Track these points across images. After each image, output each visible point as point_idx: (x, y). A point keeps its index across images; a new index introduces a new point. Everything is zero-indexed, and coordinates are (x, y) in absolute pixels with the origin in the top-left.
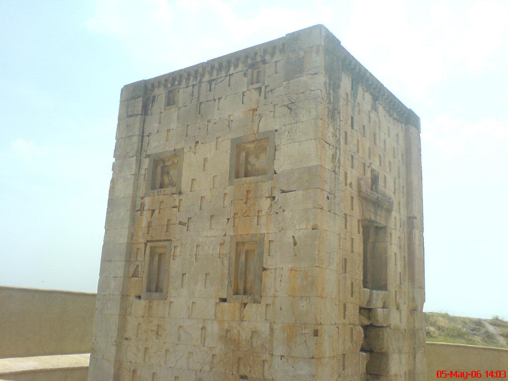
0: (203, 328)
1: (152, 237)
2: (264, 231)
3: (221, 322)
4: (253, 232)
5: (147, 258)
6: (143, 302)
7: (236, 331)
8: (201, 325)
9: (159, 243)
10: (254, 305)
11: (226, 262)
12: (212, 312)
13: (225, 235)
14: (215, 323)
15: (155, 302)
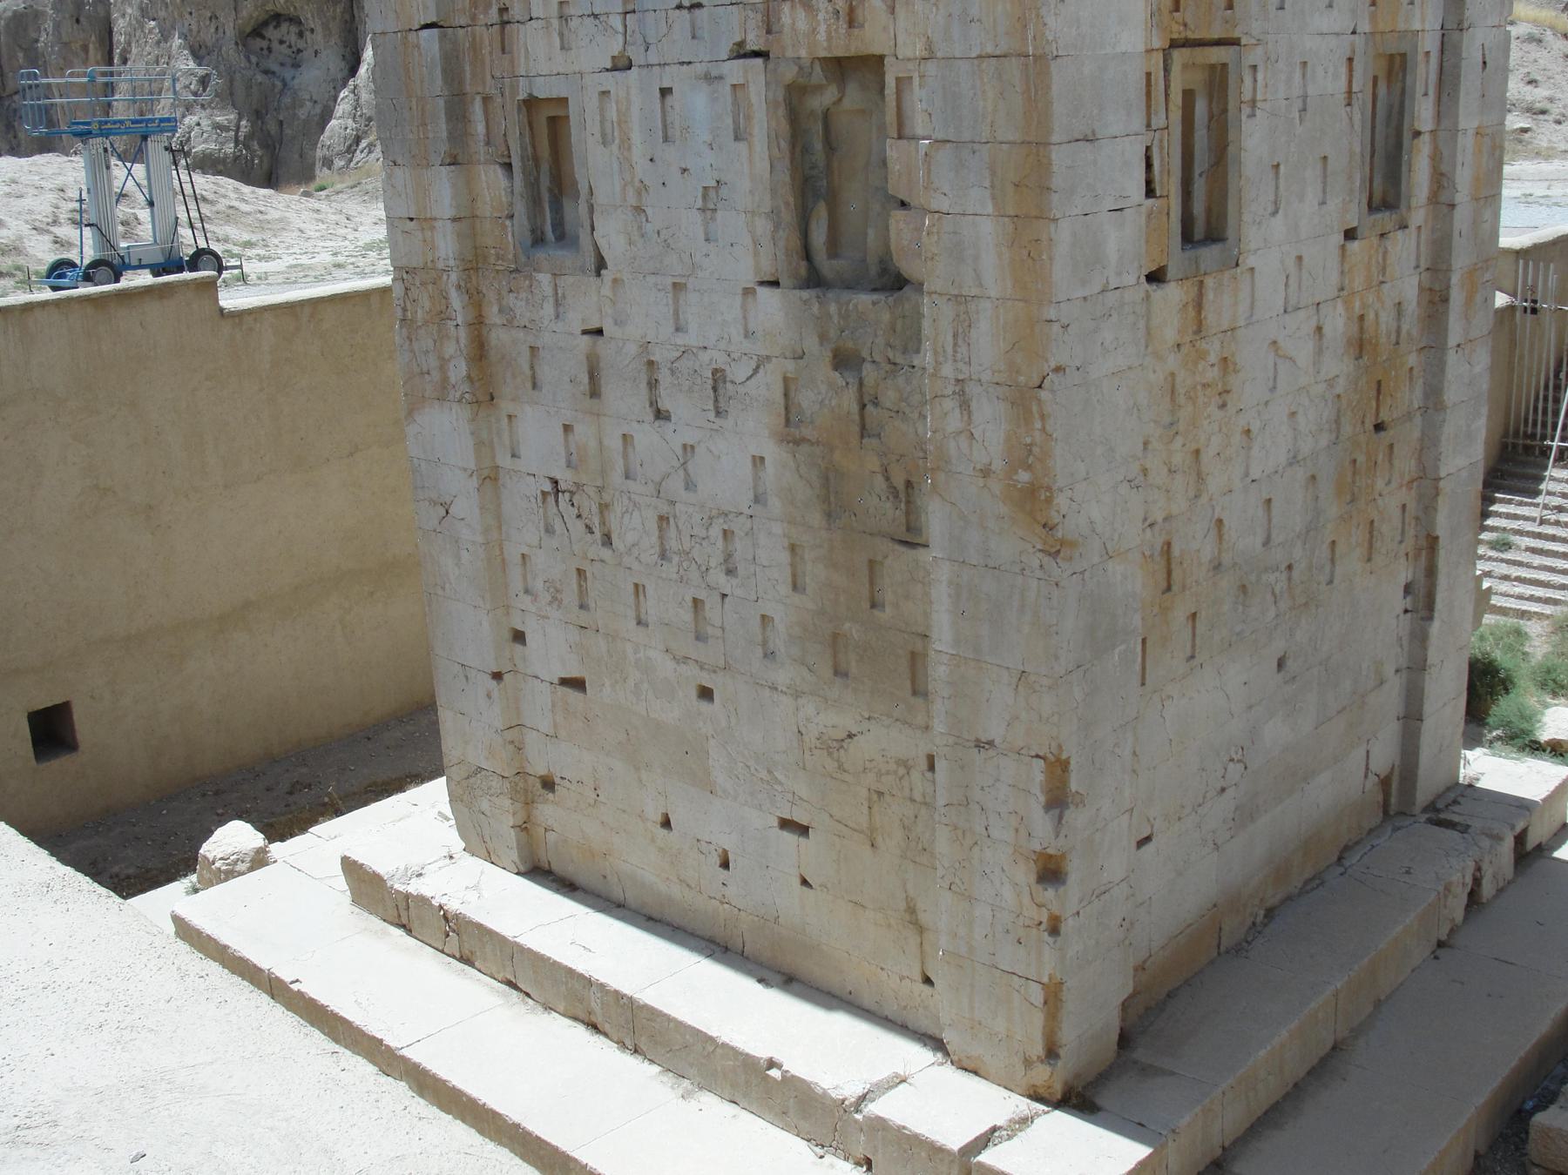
0: (1319, 329)
1: (1185, 25)
2: (1417, 26)
3: (1348, 304)
4: (1401, 26)
5: (1176, 115)
6: (1173, 294)
7: (1372, 316)
8: (1313, 323)
9: (1198, 50)
10: (1400, 233)
11: (1357, 117)
12: (1334, 278)
13: (1354, 33)
14: (1340, 308)
15: (1210, 282)
